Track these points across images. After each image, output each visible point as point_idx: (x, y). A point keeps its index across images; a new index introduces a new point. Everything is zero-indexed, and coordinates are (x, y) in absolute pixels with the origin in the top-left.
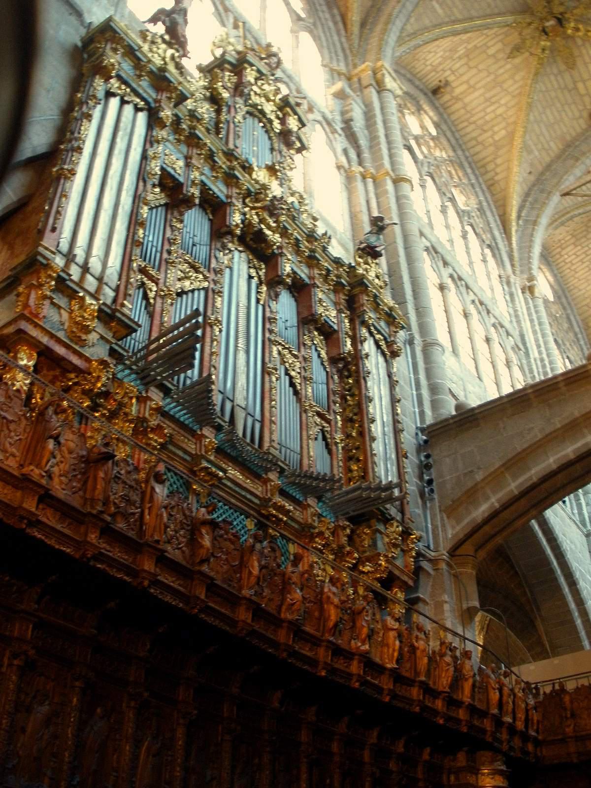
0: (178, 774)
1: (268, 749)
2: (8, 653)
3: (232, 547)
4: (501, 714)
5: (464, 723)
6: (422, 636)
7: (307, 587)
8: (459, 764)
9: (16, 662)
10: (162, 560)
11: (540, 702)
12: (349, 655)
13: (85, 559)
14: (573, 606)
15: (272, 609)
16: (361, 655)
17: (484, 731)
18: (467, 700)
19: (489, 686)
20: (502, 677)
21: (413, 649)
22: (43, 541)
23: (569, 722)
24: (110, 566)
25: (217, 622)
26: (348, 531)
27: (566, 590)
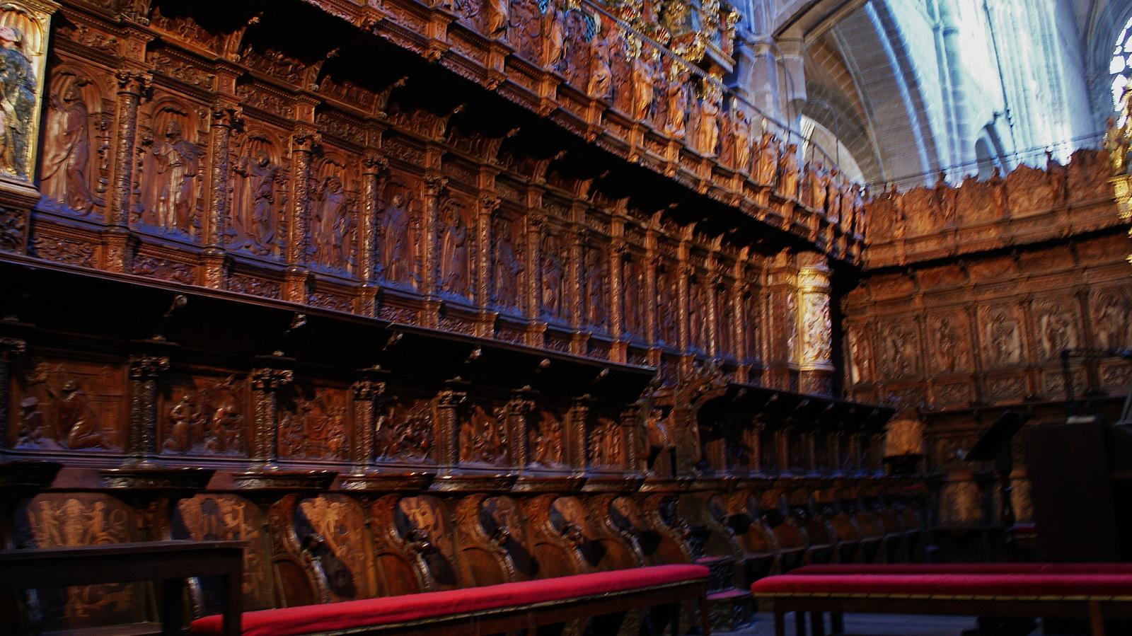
0: (484, 264)
1: (577, 242)
2: (291, 138)
3: (531, 15)
5: (785, 221)
6: (742, 124)
7: (616, 63)
8: (778, 265)
9: (301, 147)
10: (454, 28)
12: (663, 142)
13: (367, 28)
14: (911, 109)
15: (577, 86)
16: (675, 141)
17: (807, 231)
20: (829, 175)
21: (733, 138)
22: (318, 7)
23: (899, 225)
24: (395, 35)
25: (517, 100)
26: (658, 8)
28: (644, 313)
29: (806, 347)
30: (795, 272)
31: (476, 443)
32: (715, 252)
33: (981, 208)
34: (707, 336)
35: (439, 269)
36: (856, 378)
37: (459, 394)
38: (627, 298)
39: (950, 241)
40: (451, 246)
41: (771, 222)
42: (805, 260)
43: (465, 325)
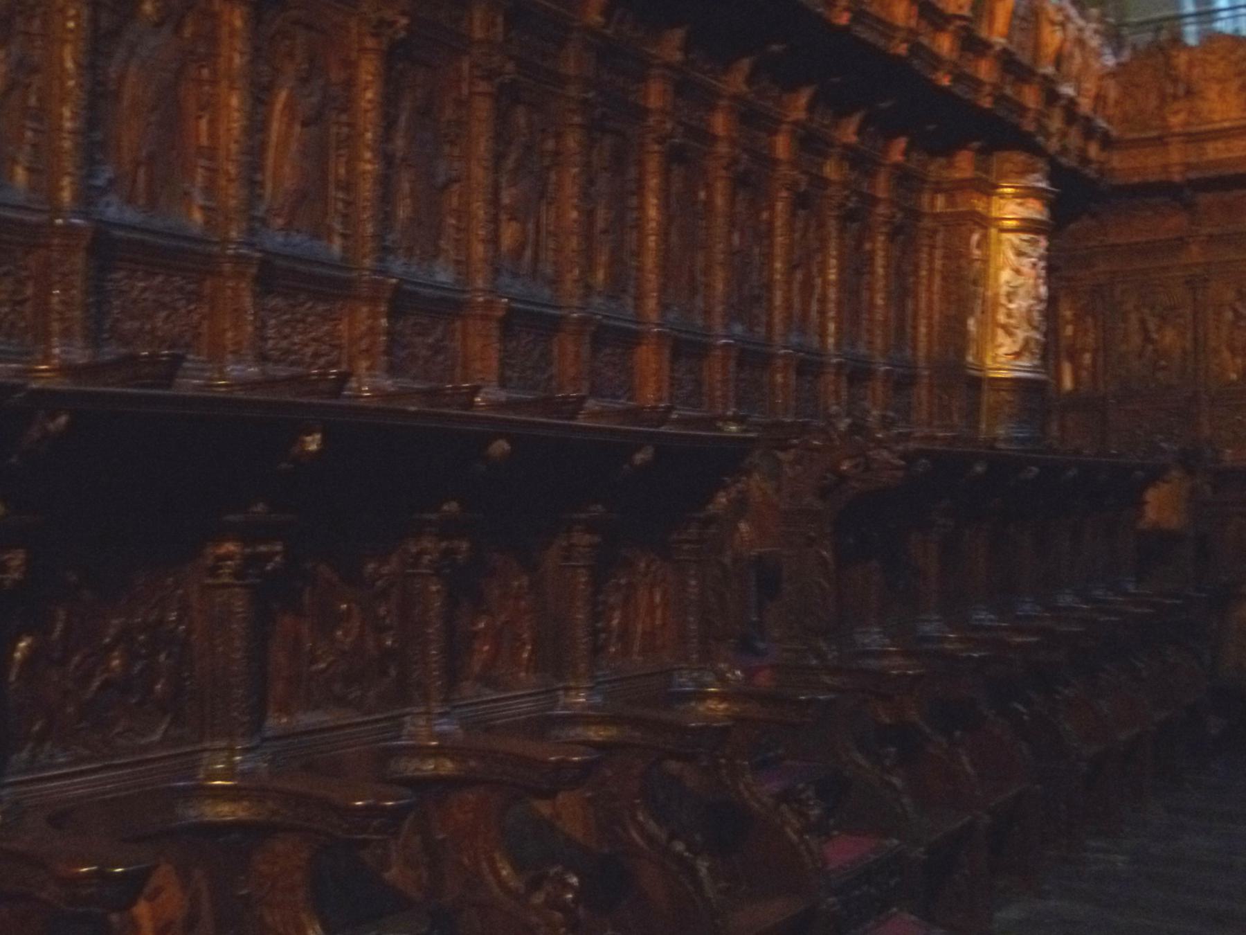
0: (368, 167)
1: (577, 119)
5: (988, 89)
17: (1022, 109)
18: (999, 40)
23: (1176, 106)
28: (707, 271)
29: (1000, 332)
30: (988, 189)
31: (314, 661)
32: (846, 146)
34: (822, 312)
35: (259, 177)
37: (263, 548)
38: (674, 239)
40: (290, 125)
41: (959, 90)
42: (1008, 166)
43: (321, 308)
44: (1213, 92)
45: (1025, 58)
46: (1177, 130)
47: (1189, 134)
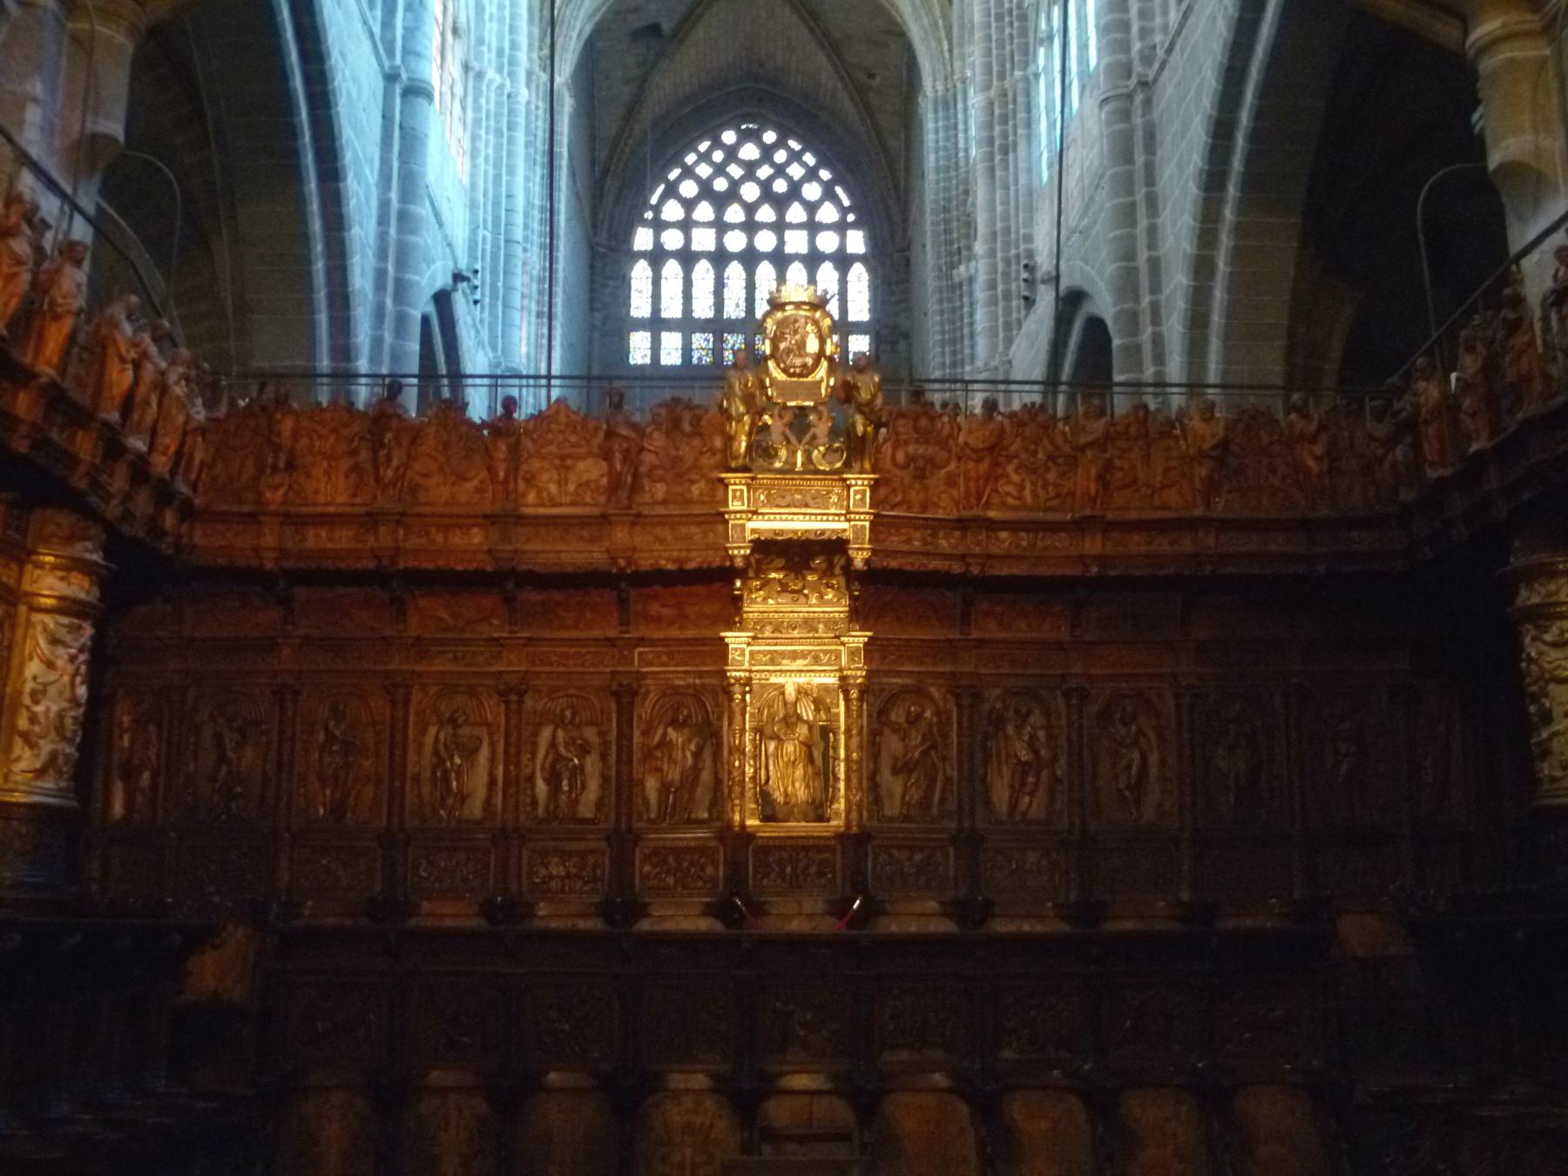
4: (123, 425)
5: (23, 429)
11: (217, 420)
14: (316, 226)
17: (73, 461)
18: (47, 371)
19: (111, 351)
23: (277, 480)
27: (312, 185)
29: (18, 743)
30: (22, 555)
33: (463, 478)
36: (118, 808)
39: (384, 537)
44: (319, 470)
45: (83, 399)
46: (273, 507)
47: (287, 515)
